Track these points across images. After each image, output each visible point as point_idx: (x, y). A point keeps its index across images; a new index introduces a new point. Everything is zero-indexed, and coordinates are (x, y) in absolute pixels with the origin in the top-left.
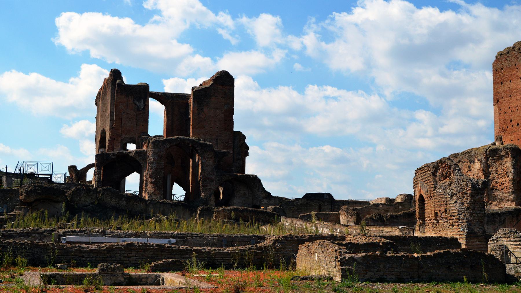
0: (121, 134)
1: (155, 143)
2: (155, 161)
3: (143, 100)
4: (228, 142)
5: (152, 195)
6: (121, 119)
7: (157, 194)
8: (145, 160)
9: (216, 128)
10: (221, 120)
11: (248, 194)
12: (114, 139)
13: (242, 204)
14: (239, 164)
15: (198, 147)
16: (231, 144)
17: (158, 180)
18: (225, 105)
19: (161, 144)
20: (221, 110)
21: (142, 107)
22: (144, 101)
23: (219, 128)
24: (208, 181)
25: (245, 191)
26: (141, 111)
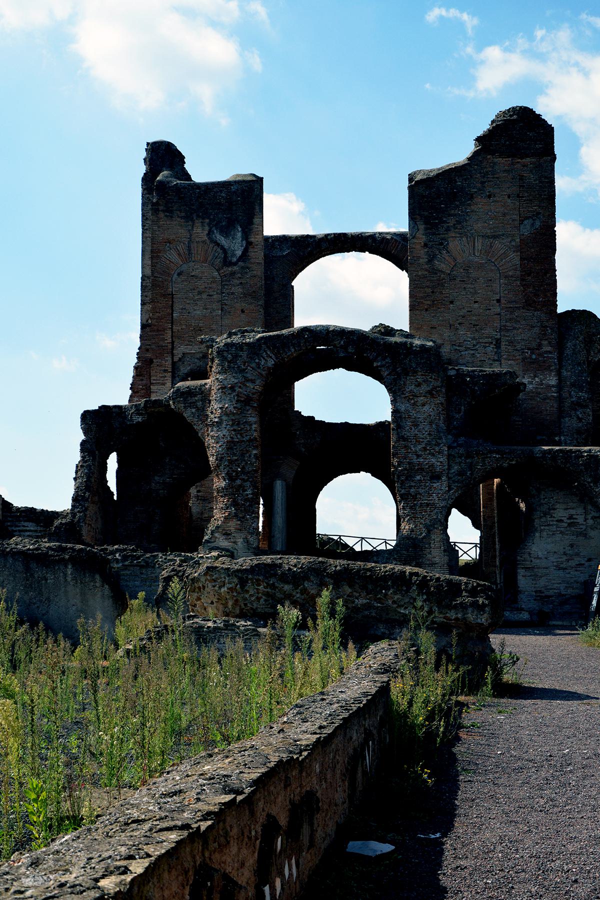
0: (173, 343)
1: (225, 354)
2: (227, 415)
3: (240, 229)
4: (540, 346)
5: (216, 535)
6: (172, 295)
7: (233, 530)
8: (202, 415)
9: (495, 302)
10: (510, 273)
11: (586, 520)
12: (151, 361)
13: (565, 558)
14: (580, 419)
15: (379, 358)
16: (550, 352)
17: (238, 482)
18: (521, 222)
19: (244, 354)
20: (510, 239)
21: (239, 253)
22: (243, 231)
23: (503, 301)
24: (418, 478)
25: (573, 512)
26: (235, 264)
